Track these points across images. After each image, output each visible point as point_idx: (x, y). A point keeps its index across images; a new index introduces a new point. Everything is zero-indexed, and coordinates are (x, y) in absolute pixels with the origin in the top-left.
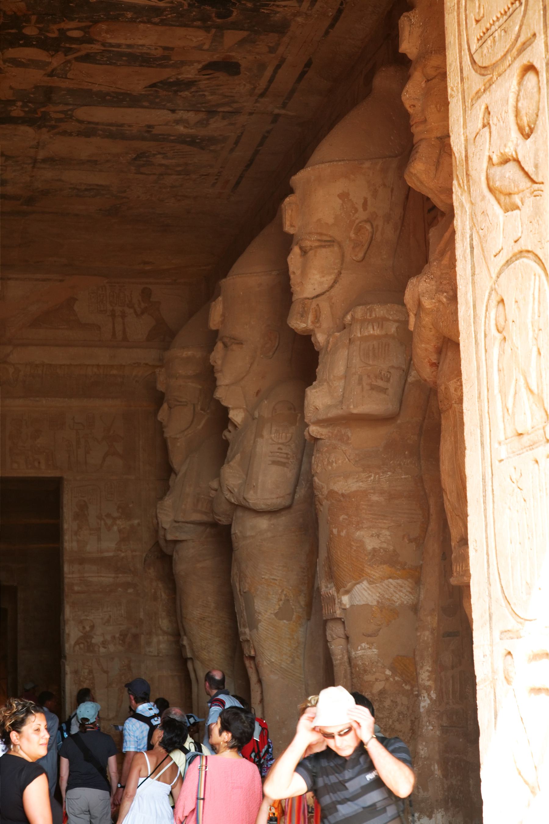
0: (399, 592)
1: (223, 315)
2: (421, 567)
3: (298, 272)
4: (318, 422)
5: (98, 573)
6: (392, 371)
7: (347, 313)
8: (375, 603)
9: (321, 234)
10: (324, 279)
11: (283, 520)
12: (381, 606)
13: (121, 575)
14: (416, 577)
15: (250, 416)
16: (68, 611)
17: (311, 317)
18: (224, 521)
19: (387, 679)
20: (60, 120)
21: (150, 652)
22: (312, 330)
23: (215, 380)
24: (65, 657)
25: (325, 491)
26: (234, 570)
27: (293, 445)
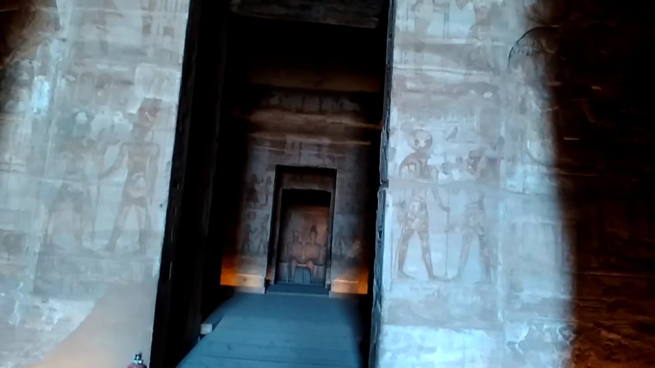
5: (442, 66)
13: (474, 72)
16: (395, 117)
21: (511, 186)
24: (386, 183)
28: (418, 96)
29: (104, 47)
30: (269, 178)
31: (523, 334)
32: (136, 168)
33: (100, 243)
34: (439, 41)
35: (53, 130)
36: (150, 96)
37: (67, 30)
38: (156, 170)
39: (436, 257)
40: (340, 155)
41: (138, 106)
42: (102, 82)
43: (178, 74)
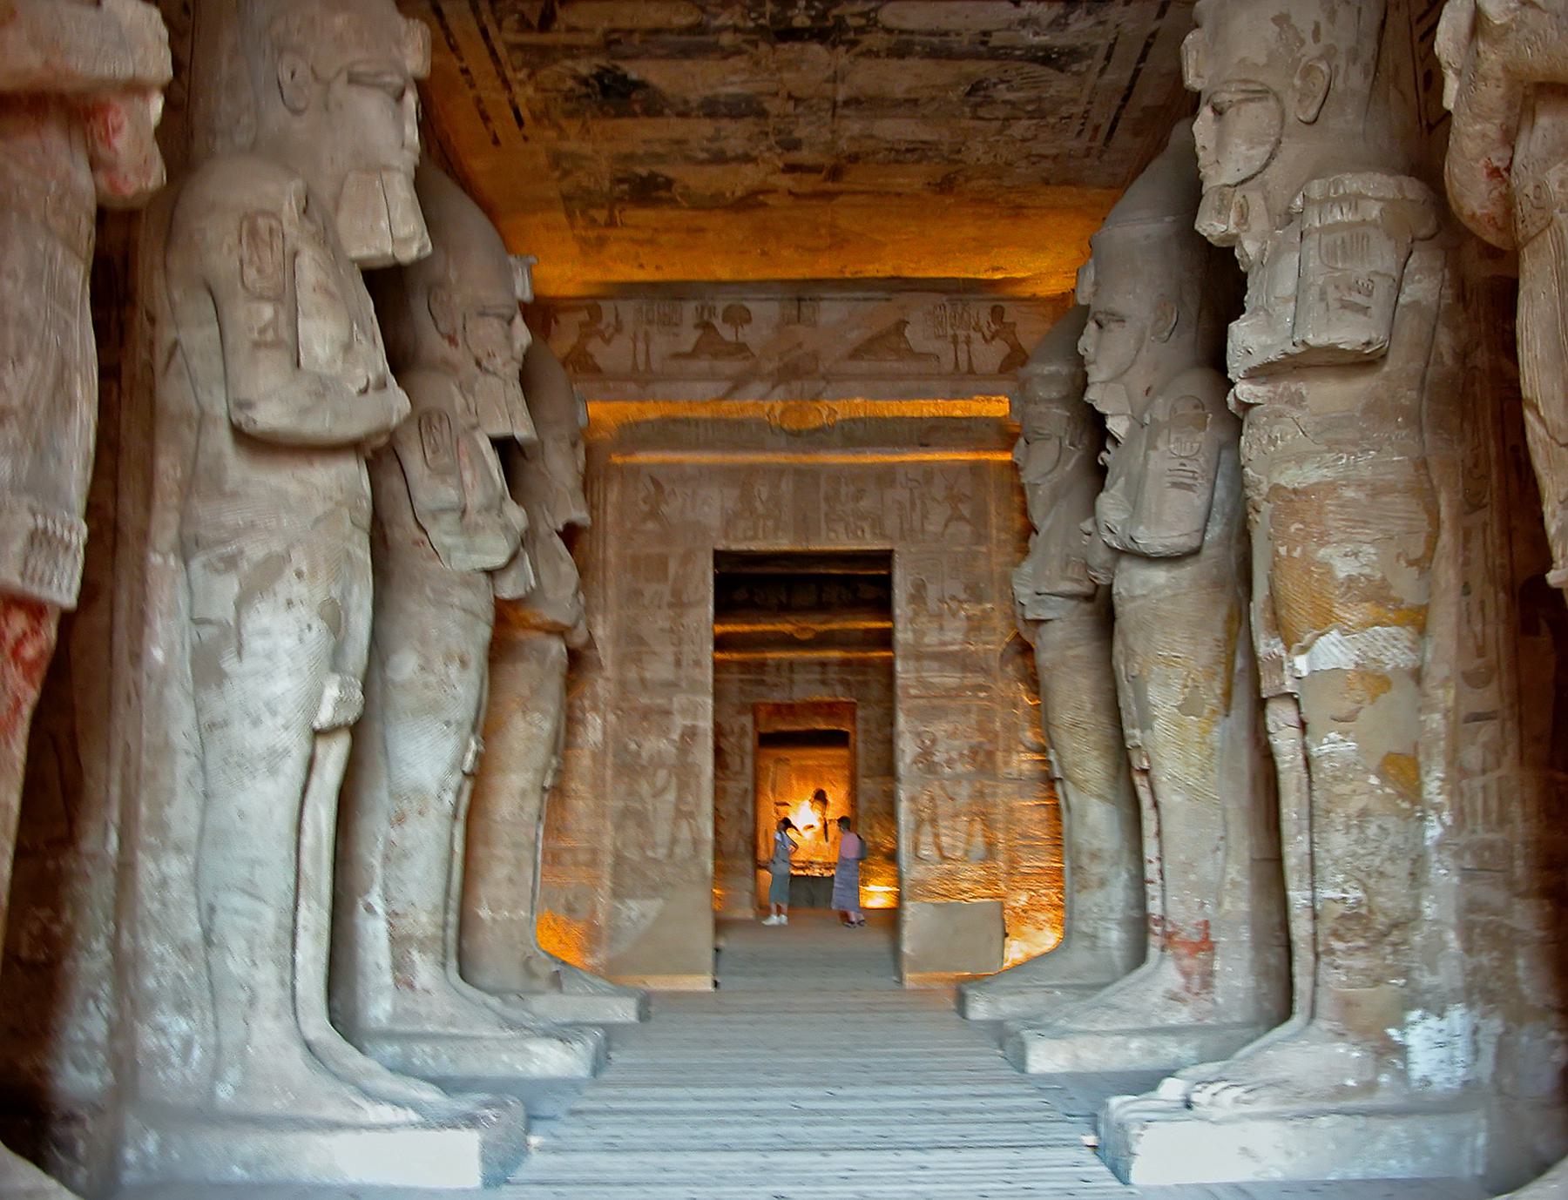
0: (1392, 648)
1: (1096, 283)
2: (1426, 607)
3: (1211, 145)
4: (1253, 375)
6: (1376, 279)
7: (1295, 195)
8: (1352, 666)
9: (1245, 81)
10: (1253, 152)
11: (1186, 572)
12: (1362, 672)
14: (1418, 621)
15: (1138, 423)
16: (902, 721)
17: (1233, 216)
18: (1102, 580)
19: (1371, 790)
20: (860, 30)
22: (1236, 236)
23: (1086, 375)
25: (1265, 488)
26: (1118, 646)
27: (1202, 460)
28: (921, 702)
29: (643, 681)
30: (743, 728)
31: (1023, 899)
32: (683, 787)
33: (661, 852)
34: (936, 649)
35: (610, 760)
36: (688, 722)
37: (610, 671)
38: (699, 785)
39: (945, 841)
40: (860, 678)
41: (679, 731)
42: (646, 714)
43: (710, 701)
